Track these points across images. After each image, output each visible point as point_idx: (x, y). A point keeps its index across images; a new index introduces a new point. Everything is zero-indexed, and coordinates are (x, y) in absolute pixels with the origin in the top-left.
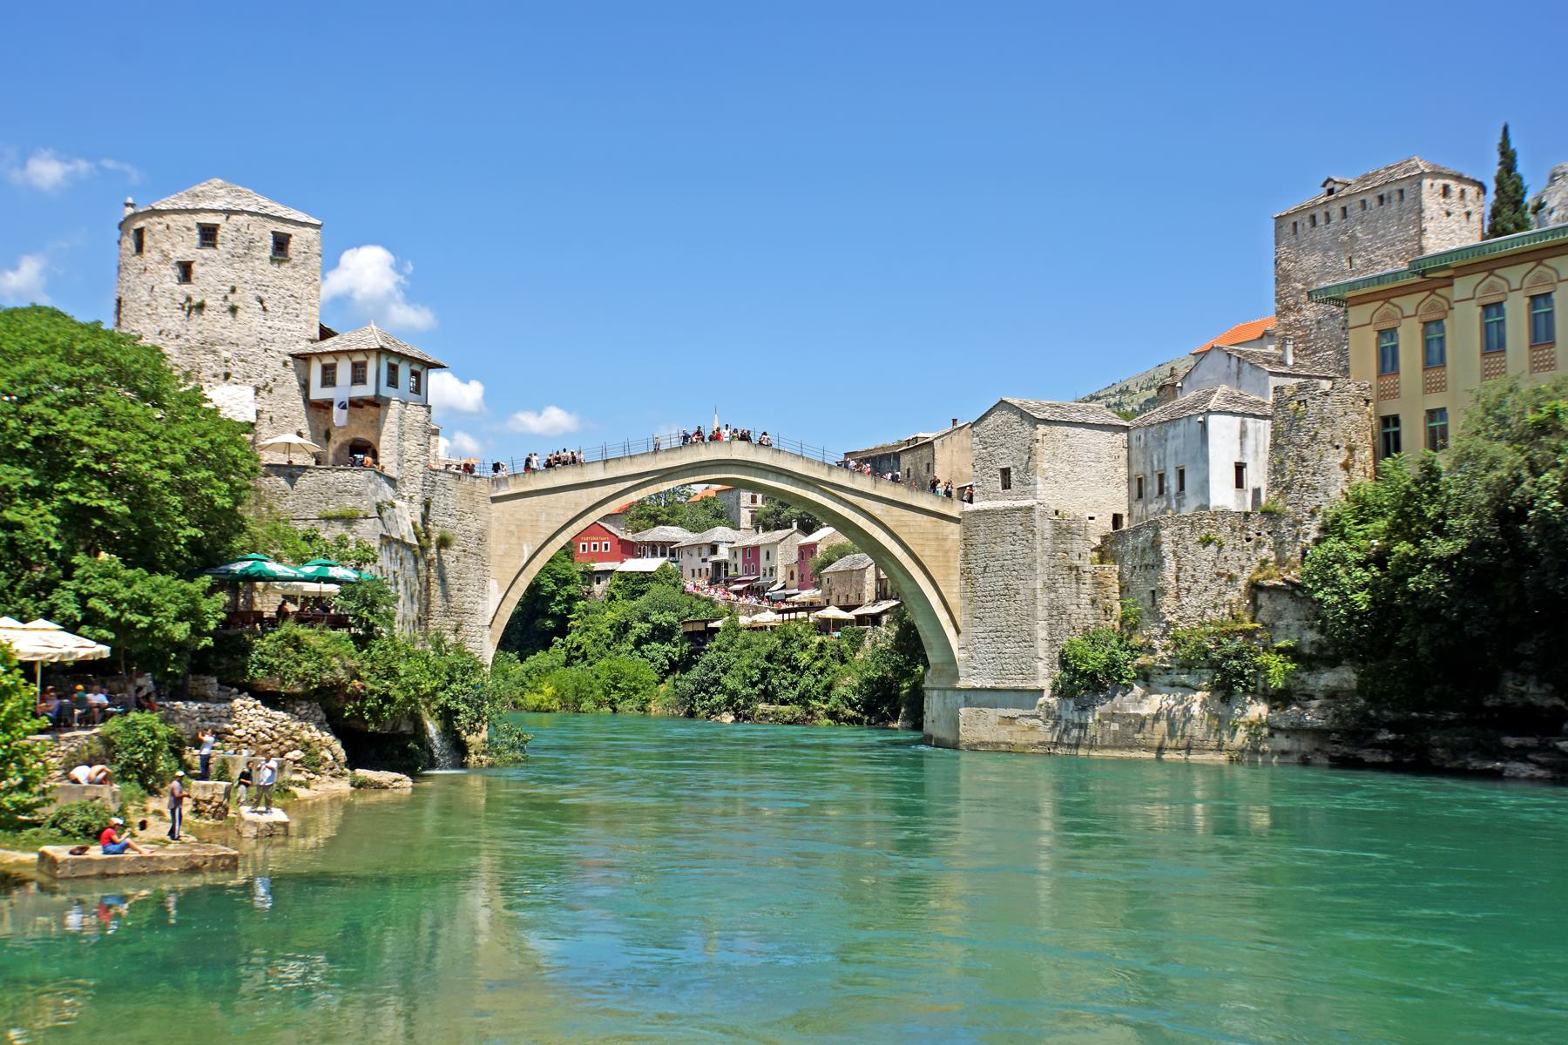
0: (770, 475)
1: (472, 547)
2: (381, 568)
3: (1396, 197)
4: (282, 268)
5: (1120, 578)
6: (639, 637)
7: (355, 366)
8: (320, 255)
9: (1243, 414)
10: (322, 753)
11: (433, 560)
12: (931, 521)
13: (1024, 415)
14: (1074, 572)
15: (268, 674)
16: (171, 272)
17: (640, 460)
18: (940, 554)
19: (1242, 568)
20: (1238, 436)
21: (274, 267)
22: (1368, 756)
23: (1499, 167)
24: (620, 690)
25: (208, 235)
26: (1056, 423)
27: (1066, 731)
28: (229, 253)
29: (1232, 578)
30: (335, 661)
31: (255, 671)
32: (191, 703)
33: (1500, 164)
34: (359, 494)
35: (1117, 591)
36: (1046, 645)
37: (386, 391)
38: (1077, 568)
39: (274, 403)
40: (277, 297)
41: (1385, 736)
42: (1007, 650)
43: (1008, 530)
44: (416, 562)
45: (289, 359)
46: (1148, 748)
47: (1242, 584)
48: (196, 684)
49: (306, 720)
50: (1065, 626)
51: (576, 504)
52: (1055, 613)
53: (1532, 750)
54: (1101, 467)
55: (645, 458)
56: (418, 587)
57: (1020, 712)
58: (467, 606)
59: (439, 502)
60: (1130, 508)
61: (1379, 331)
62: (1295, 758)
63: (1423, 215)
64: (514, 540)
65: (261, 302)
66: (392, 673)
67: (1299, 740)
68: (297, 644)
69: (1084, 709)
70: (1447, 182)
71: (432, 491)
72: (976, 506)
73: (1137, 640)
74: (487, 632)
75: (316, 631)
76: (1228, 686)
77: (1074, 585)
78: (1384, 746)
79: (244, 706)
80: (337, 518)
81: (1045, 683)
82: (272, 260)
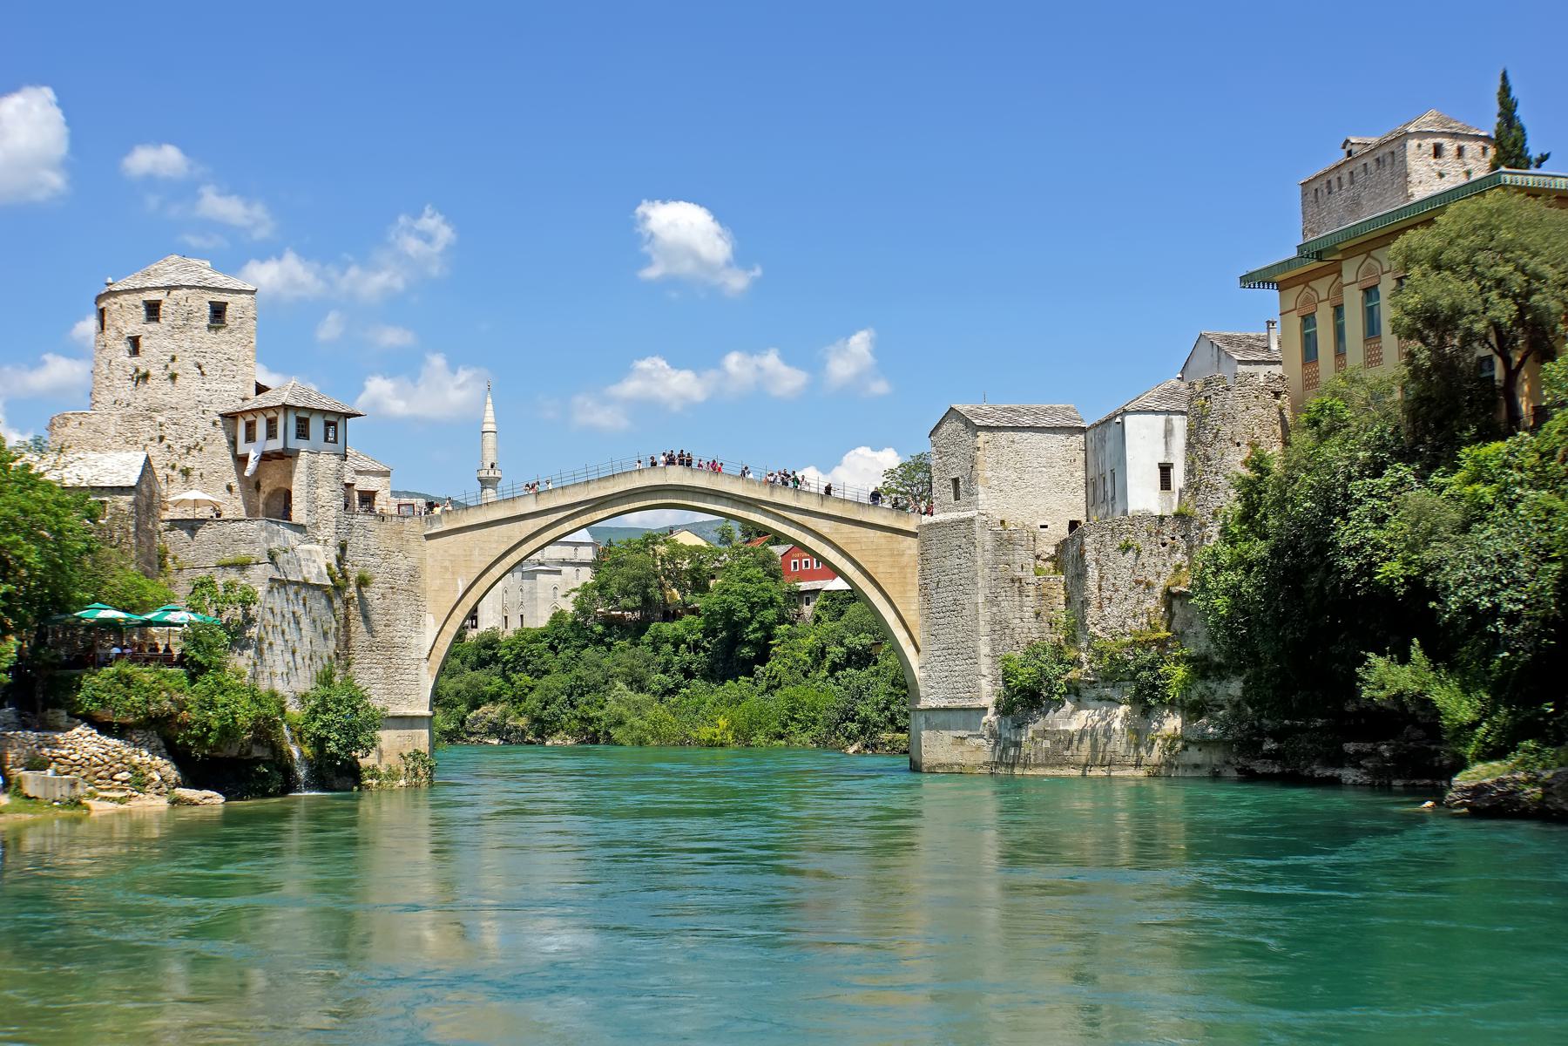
0: (709, 499)
1: (402, 583)
2: (271, 609)
3: (1389, 160)
4: (219, 334)
5: (1065, 589)
6: (833, 662)
7: (299, 420)
8: (255, 319)
9: (1168, 412)
10: (150, 775)
11: (353, 598)
12: (885, 537)
13: (968, 424)
14: (1017, 585)
15: (102, 707)
16: (123, 347)
17: (572, 490)
18: (896, 570)
19: (1159, 575)
20: (1163, 435)
21: (212, 334)
22: (1259, 767)
23: (1498, 119)
24: (799, 721)
25: (153, 310)
26: (999, 429)
27: (1005, 750)
28: (170, 325)
29: (1149, 586)
30: (164, 694)
31: (90, 705)
32: (29, 732)
33: (1499, 115)
34: (252, 542)
35: (1063, 602)
36: (989, 661)
37: (294, 443)
38: (1020, 580)
39: (205, 460)
40: (214, 361)
41: (1269, 745)
42: (957, 668)
43: (954, 543)
44: (330, 601)
45: (219, 418)
46: (1076, 765)
47: (1158, 592)
48: (53, 716)
49: (141, 746)
50: (1008, 641)
51: (509, 538)
52: (998, 627)
53: (1366, 755)
54: (1055, 472)
55: (577, 489)
56: (334, 625)
57: (968, 733)
58: (396, 640)
59: (356, 543)
60: (1087, 515)
61: (1302, 317)
62: (1205, 772)
63: (1409, 179)
64: (448, 576)
65: (200, 367)
66: (212, 705)
67: (1210, 753)
68: (128, 681)
69: (1019, 727)
70: (1439, 140)
71: (349, 533)
72: (938, 517)
73: (1071, 654)
74: (424, 665)
75: (152, 668)
76: (1148, 700)
77: (1017, 598)
78: (1270, 755)
79: (80, 734)
80: (232, 565)
81: (988, 701)
82: (210, 328)
